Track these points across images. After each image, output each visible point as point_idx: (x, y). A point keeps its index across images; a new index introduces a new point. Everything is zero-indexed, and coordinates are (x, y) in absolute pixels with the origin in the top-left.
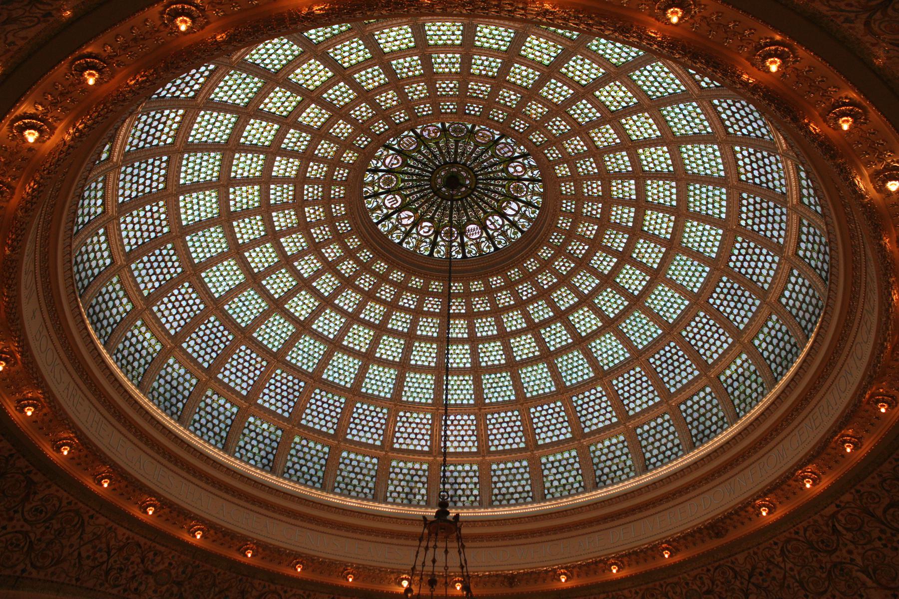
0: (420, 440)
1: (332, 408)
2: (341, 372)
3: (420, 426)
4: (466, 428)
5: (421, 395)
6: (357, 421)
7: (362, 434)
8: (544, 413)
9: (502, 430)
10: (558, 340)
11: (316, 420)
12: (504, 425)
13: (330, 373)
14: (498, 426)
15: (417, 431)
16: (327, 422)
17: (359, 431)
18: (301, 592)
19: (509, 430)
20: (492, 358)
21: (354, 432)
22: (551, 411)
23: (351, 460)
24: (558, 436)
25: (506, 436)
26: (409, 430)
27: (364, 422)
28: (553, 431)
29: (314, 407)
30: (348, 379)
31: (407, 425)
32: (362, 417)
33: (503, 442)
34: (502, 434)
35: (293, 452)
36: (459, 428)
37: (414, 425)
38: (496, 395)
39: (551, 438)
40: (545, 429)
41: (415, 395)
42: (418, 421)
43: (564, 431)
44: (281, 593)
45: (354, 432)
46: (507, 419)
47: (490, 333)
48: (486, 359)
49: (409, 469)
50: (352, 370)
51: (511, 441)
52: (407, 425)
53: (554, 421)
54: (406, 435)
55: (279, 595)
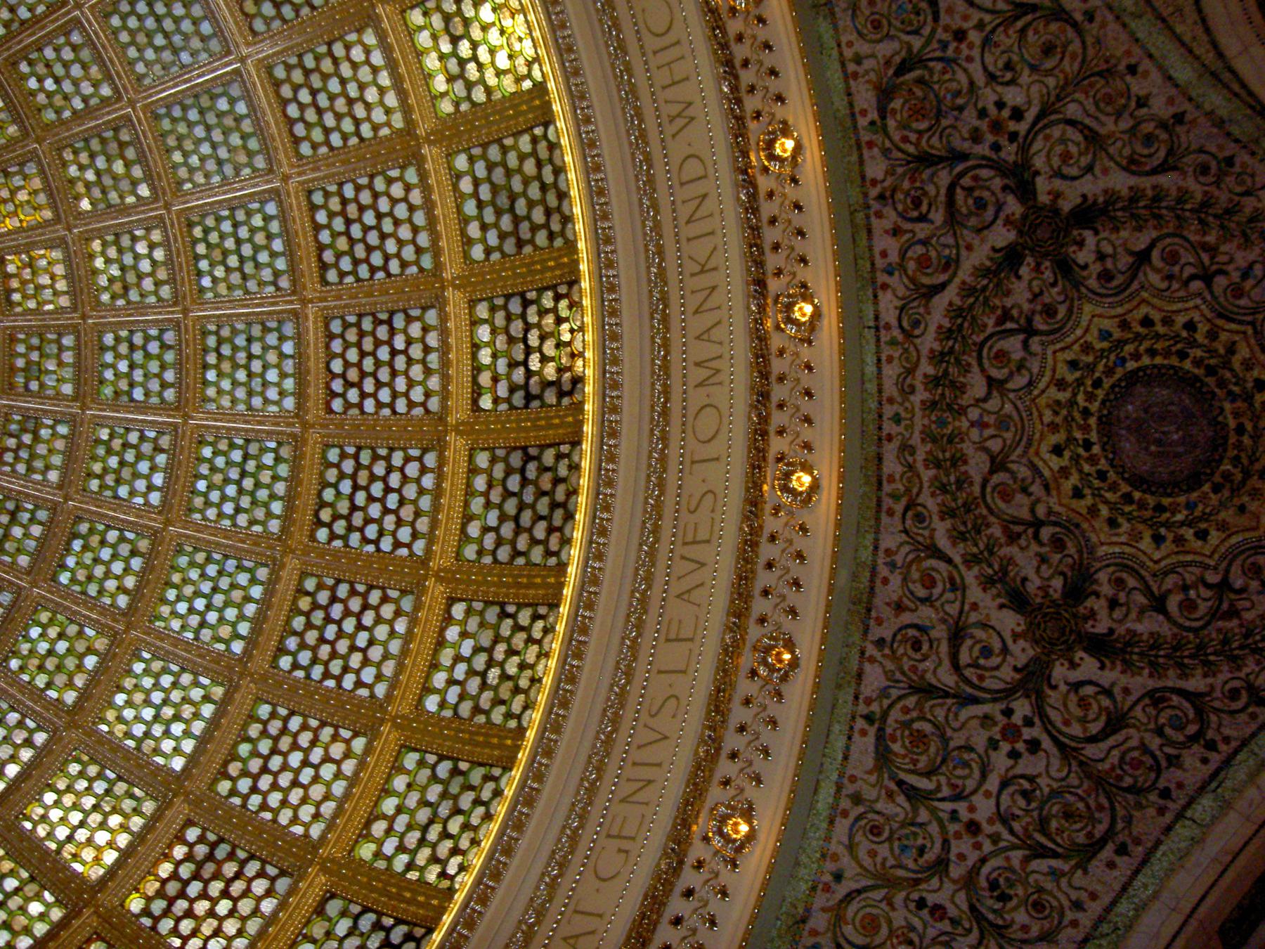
0: (405, 479)
1: (285, 743)
2: (168, 712)
3: (363, 478)
4: (368, 344)
5: (265, 477)
6: (336, 667)
7: (375, 653)
8: (311, 115)
9: (373, 238)
10: (76, 71)
11: (317, 792)
12: (356, 231)
13: (167, 745)
14: (360, 251)
15: (377, 489)
16: (327, 759)
17: (366, 662)
18: (842, 826)
19: (369, 218)
20: (145, 266)
21: (368, 675)
22: (305, 96)
23: (451, 682)
24: (375, 70)
25: (387, 226)
26: (375, 510)
27: (342, 646)
28: (362, 87)
29: (274, 799)
30: (196, 694)
31: (358, 519)
32: (325, 650)
33: (405, 232)
34: (383, 237)
35: (401, 861)
36: (368, 364)
37: (360, 498)
38: (263, 257)
39: (382, 91)
40: (360, 111)
41: (263, 494)
42: (346, 486)
43: (357, 54)
44: (841, 890)
45: (368, 675)
46: (339, 224)
47: (59, 270)
48: (148, 284)
49: (488, 505)
50: (166, 680)
51: (401, 211)
52: (358, 519)
53: (334, 85)
54: (389, 521)
55: (849, 897)
